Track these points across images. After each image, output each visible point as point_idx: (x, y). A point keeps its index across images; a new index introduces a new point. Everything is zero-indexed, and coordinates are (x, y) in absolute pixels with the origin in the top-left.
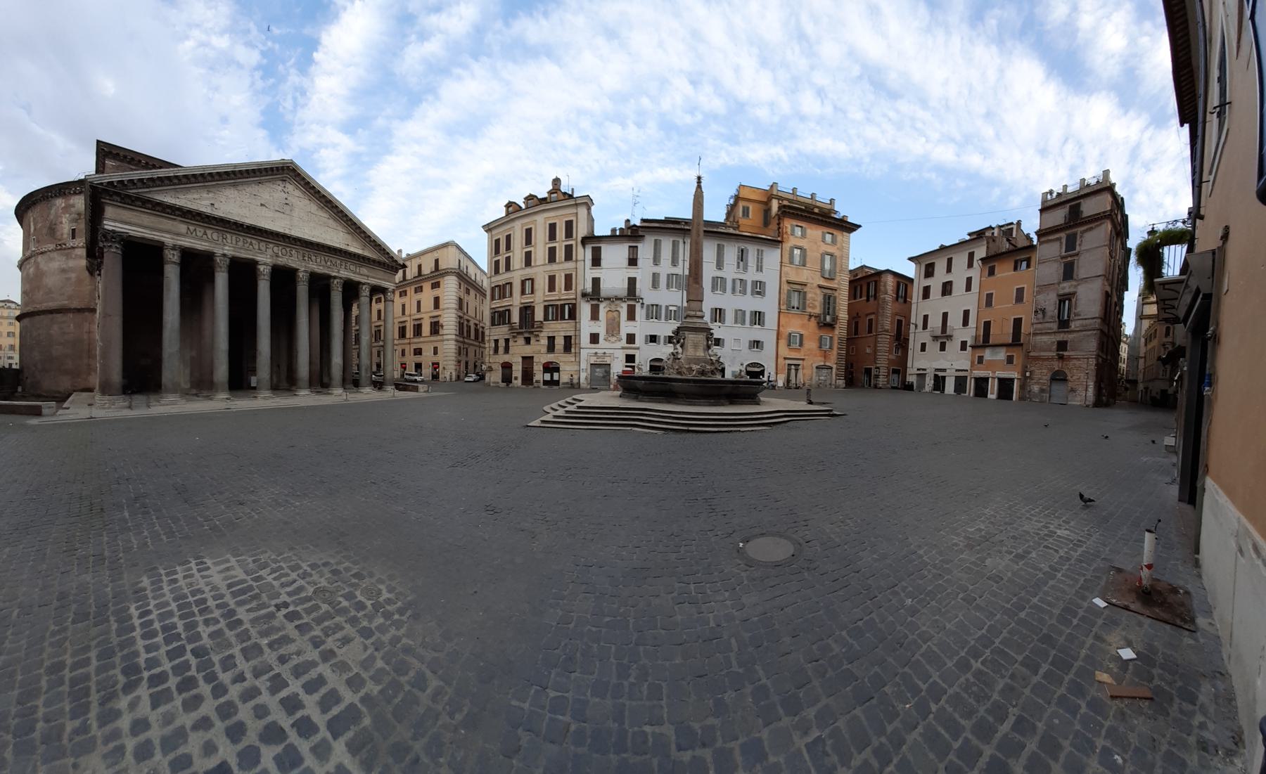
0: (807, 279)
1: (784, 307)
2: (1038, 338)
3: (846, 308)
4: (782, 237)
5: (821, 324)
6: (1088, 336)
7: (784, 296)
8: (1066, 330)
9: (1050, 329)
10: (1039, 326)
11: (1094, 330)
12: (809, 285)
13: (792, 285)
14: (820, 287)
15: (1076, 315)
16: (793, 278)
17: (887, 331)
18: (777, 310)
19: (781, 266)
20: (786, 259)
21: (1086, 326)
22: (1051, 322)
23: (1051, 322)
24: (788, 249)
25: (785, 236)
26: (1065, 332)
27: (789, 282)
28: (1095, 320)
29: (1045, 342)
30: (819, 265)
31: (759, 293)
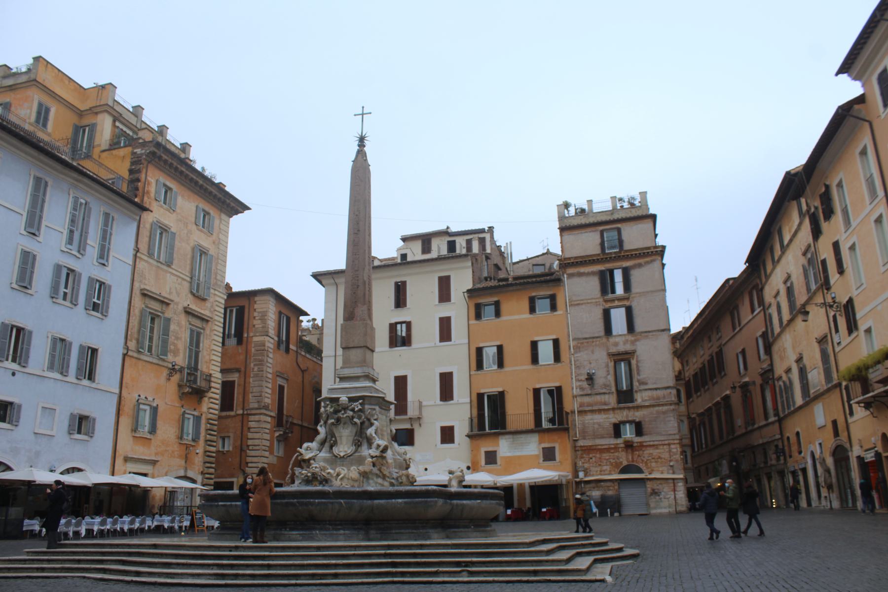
0: (170, 293)
1: (132, 345)
2: (588, 418)
3: (219, 359)
4: (142, 200)
5: (187, 390)
6: (664, 413)
7: (135, 322)
8: (630, 405)
9: (605, 404)
10: (587, 400)
11: (671, 404)
12: (171, 306)
13: (148, 301)
14: (188, 312)
15: (642, 383)
16: (152, 287)
17: (266, 407)
18: (121, 351)
19: (135, 256)
20: (143, 247)
21: (658, 398)
22: (604, 393)
23: (604, 393)
24: (148, 226)
25: (146, 198)
26: (629, 408)
27: (145, 295)
28: (669, 391)
29: (599, 424)
30: (188, 268)
31: (95, 307)
